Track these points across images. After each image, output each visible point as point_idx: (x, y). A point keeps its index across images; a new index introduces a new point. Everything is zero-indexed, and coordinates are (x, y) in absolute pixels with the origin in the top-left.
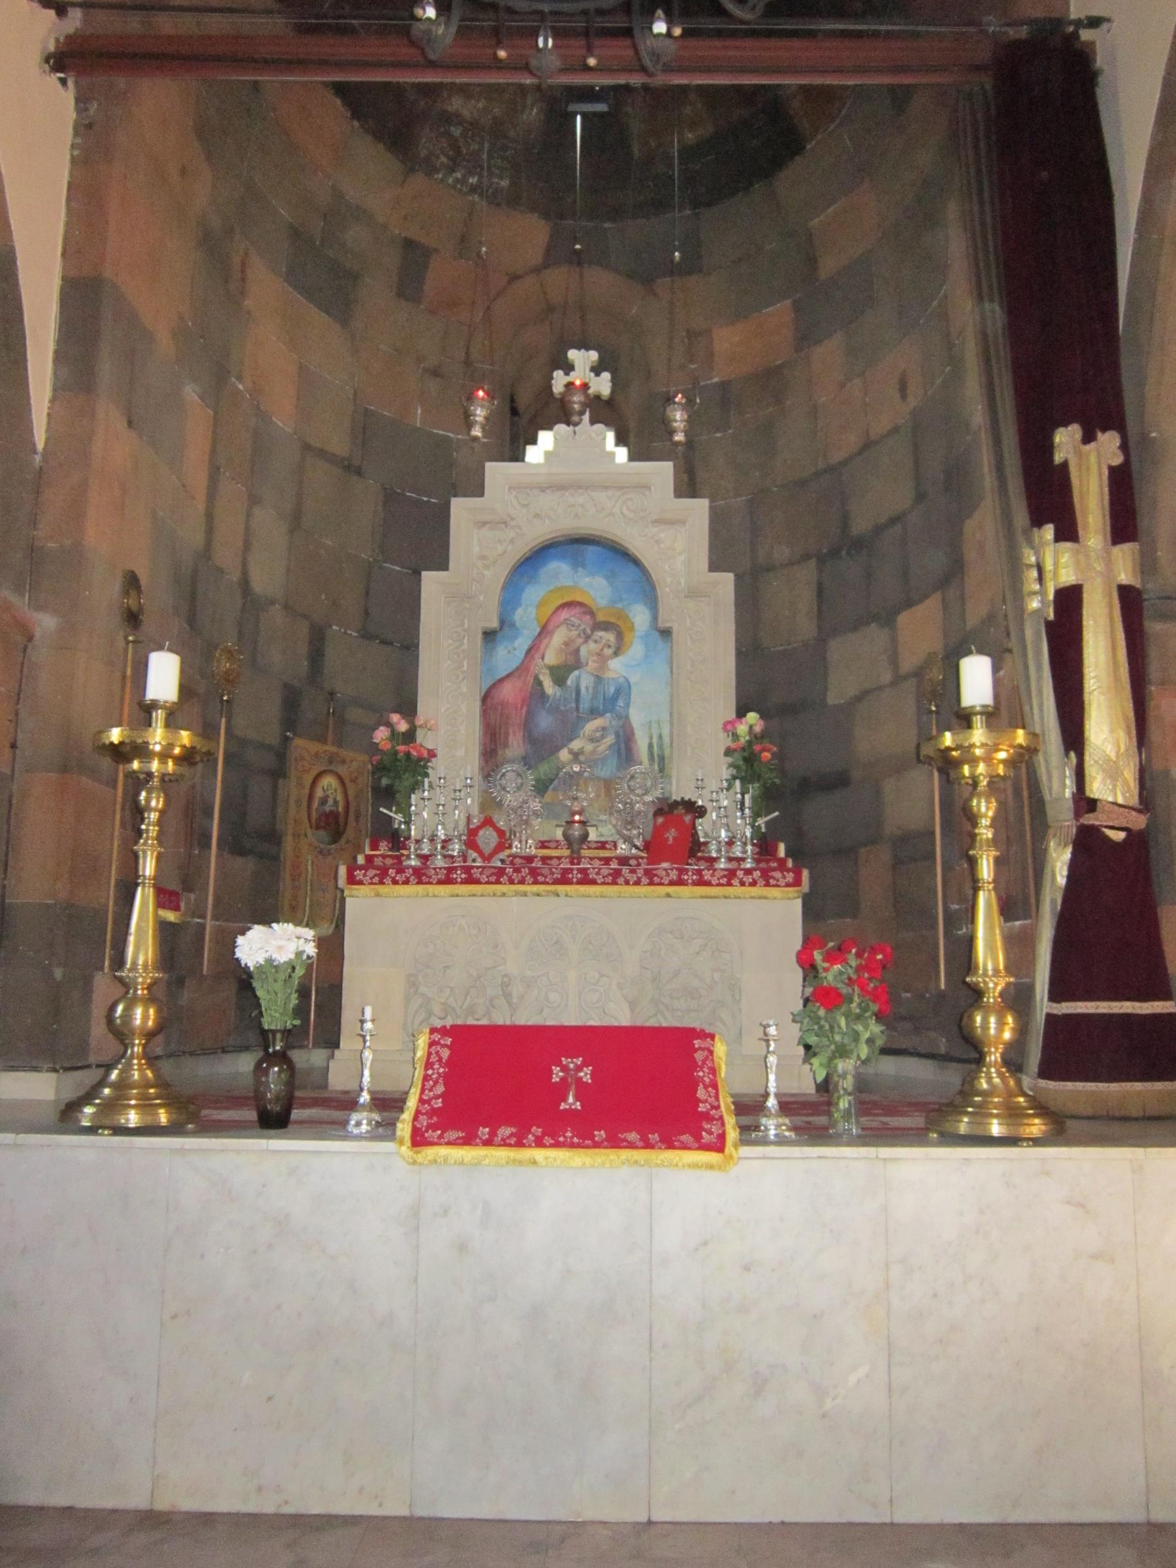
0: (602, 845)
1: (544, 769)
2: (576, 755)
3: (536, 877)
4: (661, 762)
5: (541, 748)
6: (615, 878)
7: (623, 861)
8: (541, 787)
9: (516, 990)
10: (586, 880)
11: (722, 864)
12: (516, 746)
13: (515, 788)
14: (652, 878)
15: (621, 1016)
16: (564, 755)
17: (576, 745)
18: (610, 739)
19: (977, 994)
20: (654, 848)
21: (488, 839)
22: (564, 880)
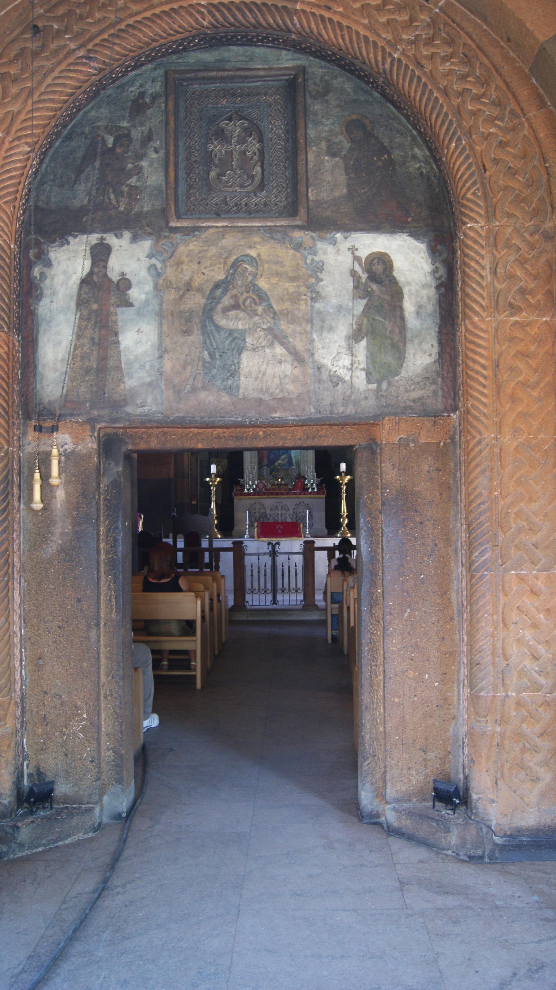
0: (285, 485)
1: (272, 467)
2: (279, 464)
3: (272, 494)
4: (298, 465)
5: (271, 462)
6: (288, 494)
7: (290, 490)
8: (271, 473)
9: (269, 517)
10: (282, 494)
11: (310, 490)
12: (265, 462)
13: (266, 471)
14: (295, 494)
15: (289, 520)
16: (276, 464)
17: (279, 461)
18: (287, 460)
19: (341, 516)
20: (295, 487)
21: (261, 486)
22: (277, 494)
